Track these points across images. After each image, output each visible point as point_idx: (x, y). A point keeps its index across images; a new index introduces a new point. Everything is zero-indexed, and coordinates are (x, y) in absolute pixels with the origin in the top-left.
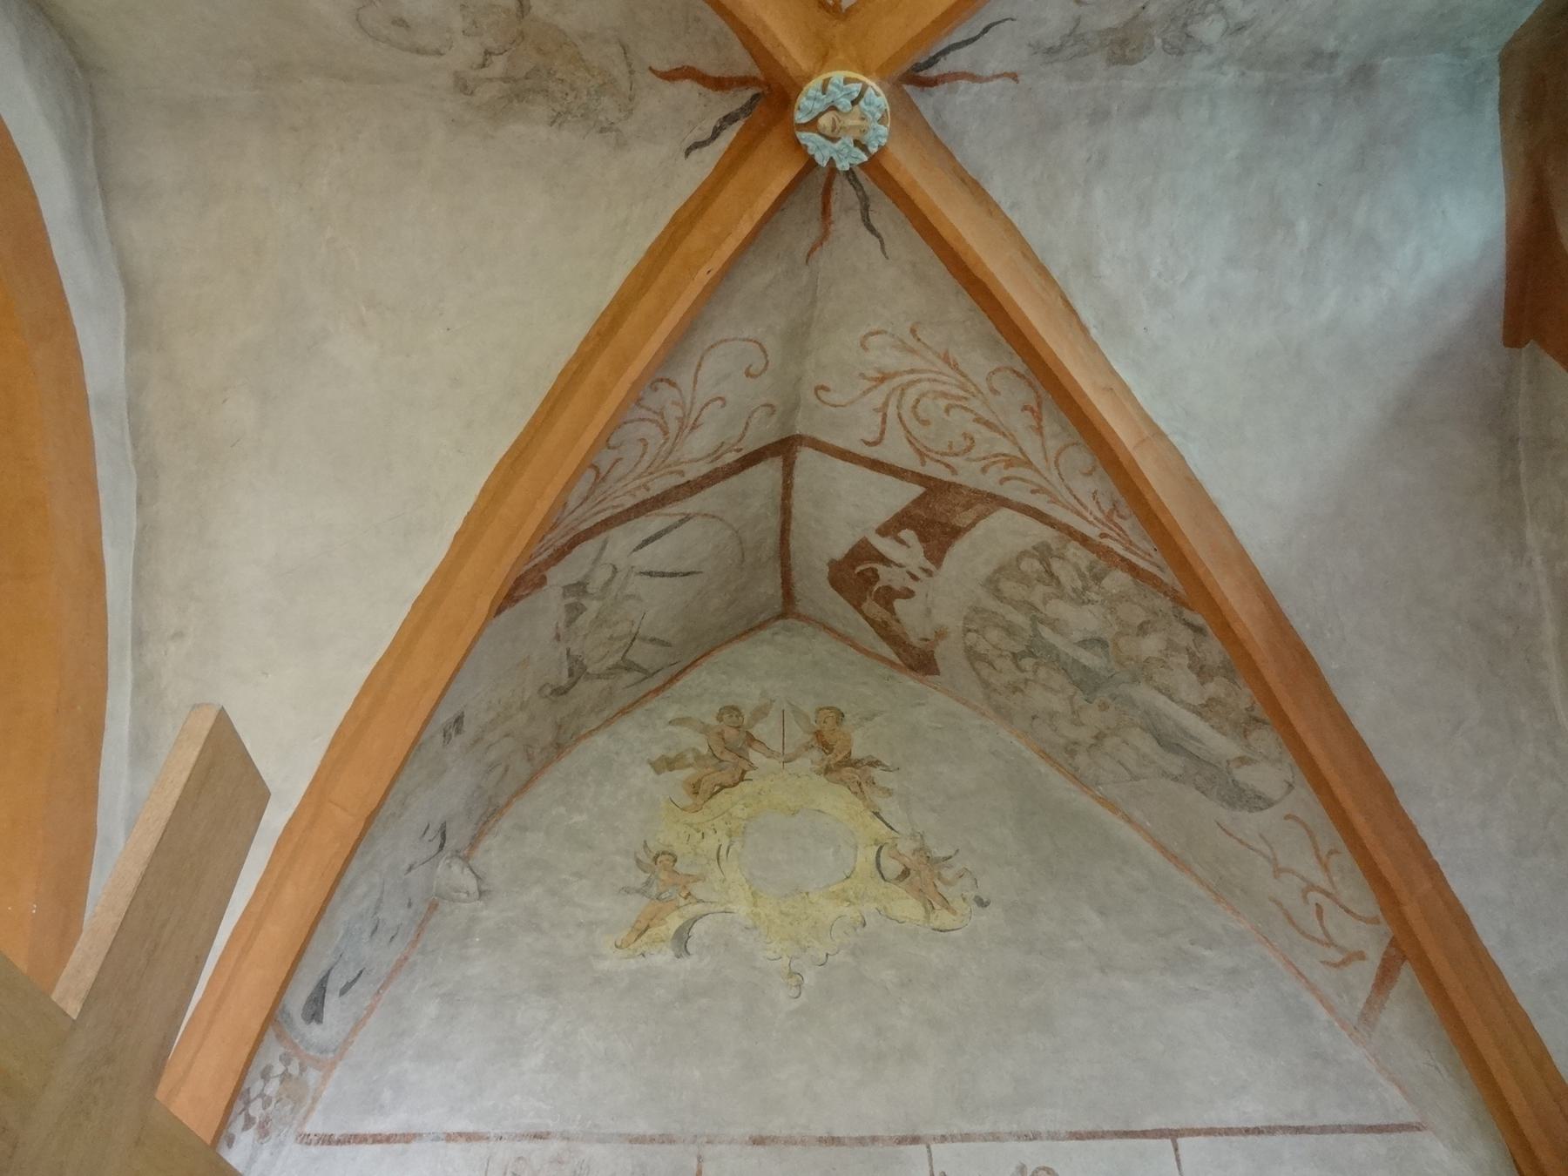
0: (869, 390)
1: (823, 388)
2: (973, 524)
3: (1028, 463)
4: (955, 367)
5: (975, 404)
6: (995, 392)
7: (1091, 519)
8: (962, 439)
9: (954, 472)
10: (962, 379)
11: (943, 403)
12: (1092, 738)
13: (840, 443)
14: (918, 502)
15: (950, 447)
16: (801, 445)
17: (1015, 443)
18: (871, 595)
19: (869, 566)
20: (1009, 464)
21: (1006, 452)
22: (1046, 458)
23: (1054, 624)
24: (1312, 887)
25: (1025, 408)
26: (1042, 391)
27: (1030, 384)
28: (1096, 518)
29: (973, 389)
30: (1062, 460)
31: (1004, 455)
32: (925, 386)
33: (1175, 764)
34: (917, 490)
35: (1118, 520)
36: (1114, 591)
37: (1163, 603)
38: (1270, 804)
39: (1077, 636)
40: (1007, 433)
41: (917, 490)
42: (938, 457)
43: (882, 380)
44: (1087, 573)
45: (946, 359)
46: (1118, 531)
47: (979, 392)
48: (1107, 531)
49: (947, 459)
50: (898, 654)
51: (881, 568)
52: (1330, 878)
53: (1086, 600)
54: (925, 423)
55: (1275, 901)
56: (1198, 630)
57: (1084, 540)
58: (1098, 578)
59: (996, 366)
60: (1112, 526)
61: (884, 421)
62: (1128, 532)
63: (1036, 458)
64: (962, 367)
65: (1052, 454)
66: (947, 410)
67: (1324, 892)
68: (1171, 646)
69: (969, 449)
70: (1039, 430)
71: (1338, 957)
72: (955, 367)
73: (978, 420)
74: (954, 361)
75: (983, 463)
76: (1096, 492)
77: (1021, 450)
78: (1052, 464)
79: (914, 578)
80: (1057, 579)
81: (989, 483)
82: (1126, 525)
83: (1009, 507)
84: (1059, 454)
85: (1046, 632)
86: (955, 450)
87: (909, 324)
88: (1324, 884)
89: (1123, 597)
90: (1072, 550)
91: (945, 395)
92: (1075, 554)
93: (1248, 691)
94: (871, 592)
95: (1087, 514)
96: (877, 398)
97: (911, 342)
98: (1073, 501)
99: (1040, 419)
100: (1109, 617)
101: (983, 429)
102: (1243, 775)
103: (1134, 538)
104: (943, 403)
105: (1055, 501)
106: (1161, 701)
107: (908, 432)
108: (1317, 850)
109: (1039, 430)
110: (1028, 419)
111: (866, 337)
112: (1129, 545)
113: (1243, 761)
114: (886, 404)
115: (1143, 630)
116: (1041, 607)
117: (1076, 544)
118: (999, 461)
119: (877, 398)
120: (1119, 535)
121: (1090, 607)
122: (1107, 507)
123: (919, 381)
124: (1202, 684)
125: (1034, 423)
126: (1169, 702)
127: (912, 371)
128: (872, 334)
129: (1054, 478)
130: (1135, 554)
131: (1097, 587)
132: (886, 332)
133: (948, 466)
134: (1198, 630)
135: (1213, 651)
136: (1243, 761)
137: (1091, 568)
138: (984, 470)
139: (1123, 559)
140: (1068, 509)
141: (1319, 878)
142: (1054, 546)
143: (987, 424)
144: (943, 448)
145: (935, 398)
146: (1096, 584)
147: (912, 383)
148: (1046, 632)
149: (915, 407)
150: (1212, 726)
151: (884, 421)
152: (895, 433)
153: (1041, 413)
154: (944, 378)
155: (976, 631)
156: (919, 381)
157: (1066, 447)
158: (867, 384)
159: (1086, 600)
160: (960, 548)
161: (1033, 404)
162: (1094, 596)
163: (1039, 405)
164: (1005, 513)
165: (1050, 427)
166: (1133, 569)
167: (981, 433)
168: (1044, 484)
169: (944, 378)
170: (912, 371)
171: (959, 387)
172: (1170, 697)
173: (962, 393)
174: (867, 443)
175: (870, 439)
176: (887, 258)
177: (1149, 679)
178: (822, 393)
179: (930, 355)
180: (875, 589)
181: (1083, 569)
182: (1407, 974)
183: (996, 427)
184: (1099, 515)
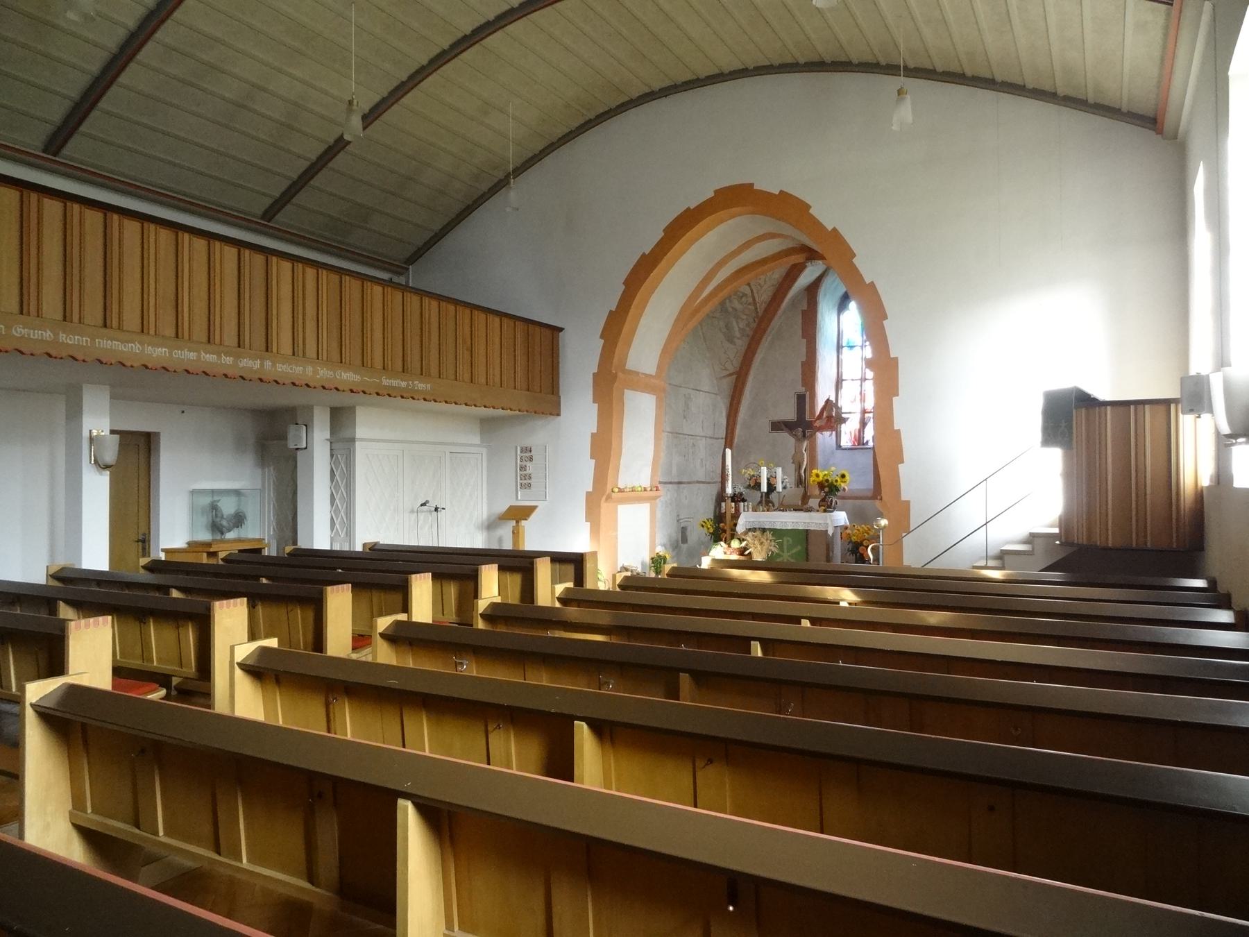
3: (761, 287)
23: (730, 301)
24: (729, 358)
33: (724, 330)
37: (754, 315)
57: (754, 300)
106: (734, 323)
115: (745, 314)
135: (754, 325)
136: (738, 338)
141: (732, 358)
182: (735, 376)
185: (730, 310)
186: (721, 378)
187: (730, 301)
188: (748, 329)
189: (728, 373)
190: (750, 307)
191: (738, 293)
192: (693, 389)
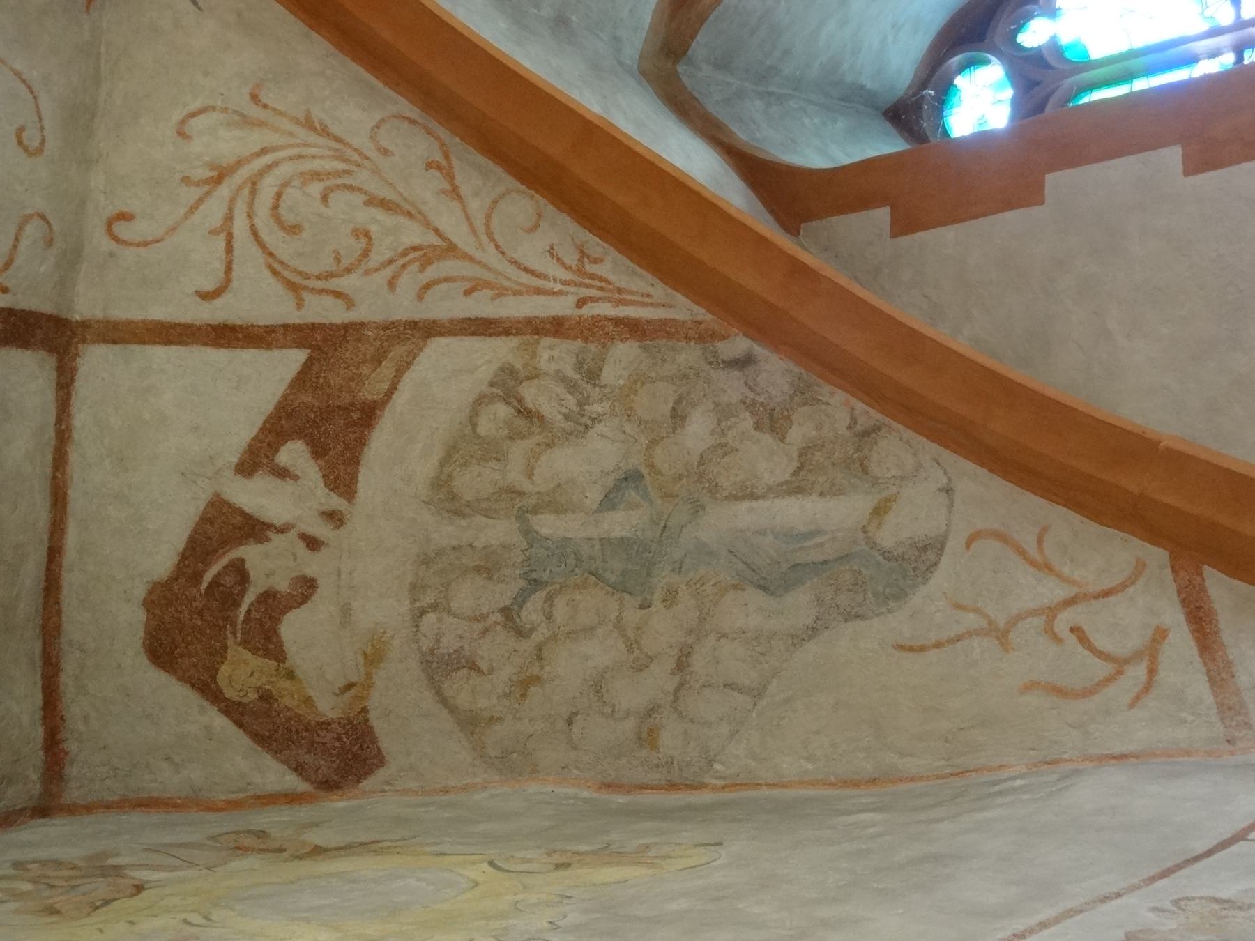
0: (200, 201)
1: (125, 217)
2: (393, 388)
3: (451, 249)
4: (325, 132)
5: (361, 177)
6: (385, 152)
7: (558, 287)
8: (352, 241)
9: (350, 303)
10: (338, 146)
11: (316, 188)
12: (673, 674)
13: (158, 313)
14: (302, 379)
15: (338, 260)
16: (84, 341)
17: (427, 224)
18: (234, 634)
19: (224, 561)
20: (426, 262)
21: (417, 241)
22: (474, 231)
23: (554, 503)
24: (1051, 612)
25: (429, 166)
26: (443, 133)
27: (429, 132)
28: (564, 283)
29: (356, 157)
30: (495, 222)
31: (415, 249)
32: (285, 170)
34: (295, 358)
35: (590, 268)
36: (621, 382)
37: (689, 355)
38: (939, 545)
39: (594, 495)
40: (413, 212)
41: (295, 358)
42: (320, 284)
43: (218, 180)
44: (577, 376)
45: (309, 124)
46: (597, 283)
47: (367, 158)
48: (585, 292)
49: (334, 284)
50: (299, 769)
51: (250, 553)
52: (1059, 576)
53: (589, 422)
54: (293, 230)
55: (1029, 687)
56: (744, 362)
57: (557, 327)
58: (593, 376)
59: (378, 116)
60: (590, 281)
61: (229, 249)
62: (611, 277)
63: (460, 235)
64: (335, 129)
65: (479, 222)
66: (324, 198)
67: (1069, 602)
68: (723, 413)
69: (366, 253)
70: (455, 193)
71: (1138, 672)
72: (325, 132)
73: (372, 201)
74: (321, 123)
75: (388, 272)
76: (552, 248)
77: (436, 231)
78: (484, 238)
79: (313, 543)
80: (540, 417)
81: (403, 307)
82: (602, 270)
83: (441, 334)
84: (488, 217)
85: (547, 525)
86: (345, 262)
87: (246, 90)
88: (1061, 592)
89: (638, 380)
90: (545, 356)
91: (316, 175)
92: (551, 359)
93: (840, 396)
94: (234, 624)
95: (549, 285)
96: (214, 210)
97: (254, 112)
98: (525, 278)
99: (450, 177)
100: (628, 428)
101: (379, 214)
102: (889, 535)
103: (621, 281)
104: (316, 188)
105: (502, 292)
106: (744, 515)
107: (271, 254)
108: (1022, 553)
109: (455, 193)
110: (437, 181)
111: (183, 122)
112: (619, 296)
113: (879, 511)
114: (229, 218)
115: (678, 417)
116: (527, 486)
117: (547, 341)
118: (410, 262)
119: (214, 210)
120: (601, 289)
121: (599, 428)
122: (571, 258)
123: (276, 164)
124: (783, 439)
125: (447, 186)
126: (754, 504)
127: (264, 151)
128: (193, 115)
129: (490, 256)
130: (632, 303)
131: (597, 389)
132: (214, 108)
133: (337, 294)
134: (744, 362)
136: (879, 511)
137: (579, 366)
138: (392, 284)
139: (617, 321)
140: (520, 293)
141: (1053, 591)
142: (519, 366)
143: (384, 204)
144: (327, 264)
145: (304, 184)
146: (595, 385)
147: (269, 167)
148: (547, 525)
149: (276, 207)
150: (821, 494)
151: (229, 249)
152: (249, 263)
153: (451, 167)
154: (312, 151)
155: (434, 607)
156: (276, 164)
157: (495, 202)
158: (195, 193)
159: (589, 422)
160: (381, 441)
161: (438, 157)
162: (597, 408)
163: (447, 157)
164: (439, 344)
165: (468, 181)
166: (634, 329)
167: (377, 220)
168: (478, 272)
169: (312, 151)
170: (264, 151)
171: (337, 158)
172: (753, 497)
173: (341, 166)
174: (206, 296)
175: (209, 286)
176: (200, 9)
177: (714, 488)
178: (121, 229)
179: (288, 125)
180: (242, 617)
181: (570, 372)
183: (397, 205)
184: (568, 276)
185: (619, 523)
186: (1229, 708)
187: (554, 503)
188: (798, 433)
189: (1181, 640)
190: (612, 374)
191: (485, 427)
192: (1152, 879)
